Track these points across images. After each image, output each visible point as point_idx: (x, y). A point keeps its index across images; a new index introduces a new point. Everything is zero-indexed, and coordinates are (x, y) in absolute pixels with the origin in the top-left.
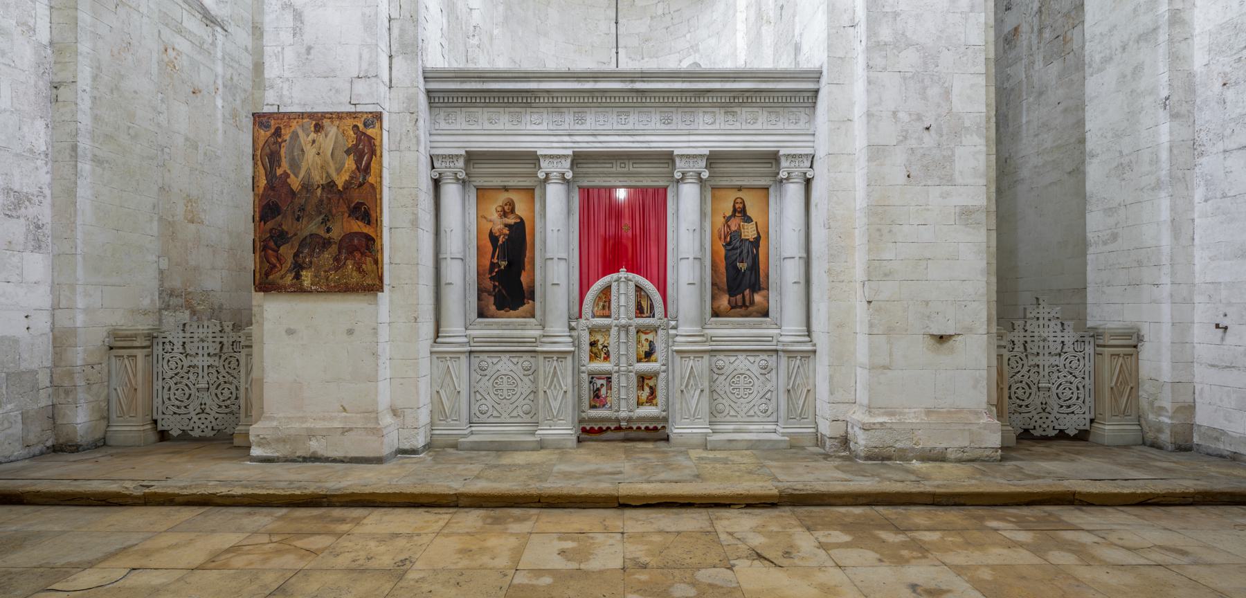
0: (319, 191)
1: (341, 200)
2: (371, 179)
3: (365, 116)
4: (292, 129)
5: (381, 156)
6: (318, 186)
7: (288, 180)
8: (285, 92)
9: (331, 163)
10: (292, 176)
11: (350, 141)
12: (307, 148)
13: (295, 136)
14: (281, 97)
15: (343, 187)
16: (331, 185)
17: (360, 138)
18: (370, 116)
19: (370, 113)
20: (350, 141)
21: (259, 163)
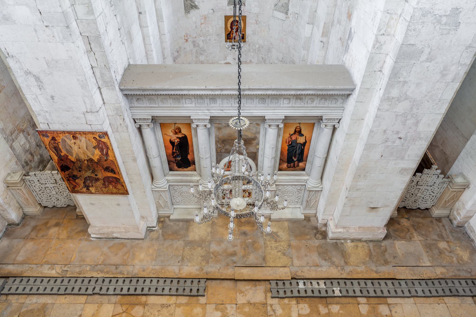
0: (86, 162)
1: (98, 166)
2: (110, 158)
3: (98, 133)
4: (61, 138)
5: (113, 150)
6: (85, 160)
7: (68, 157)
8: (48, 117)
9: (88, 152)
10: (69, 156)
11: (94, 143)
12: (73, 145)
13: (64, 141)
14: (47, 119)
15: (97, 160)
16: (91, 160)
17: (99, 143)
18: (101, 133)
19: (101, 132)
20: (94, 143)
21: (50, 150)
